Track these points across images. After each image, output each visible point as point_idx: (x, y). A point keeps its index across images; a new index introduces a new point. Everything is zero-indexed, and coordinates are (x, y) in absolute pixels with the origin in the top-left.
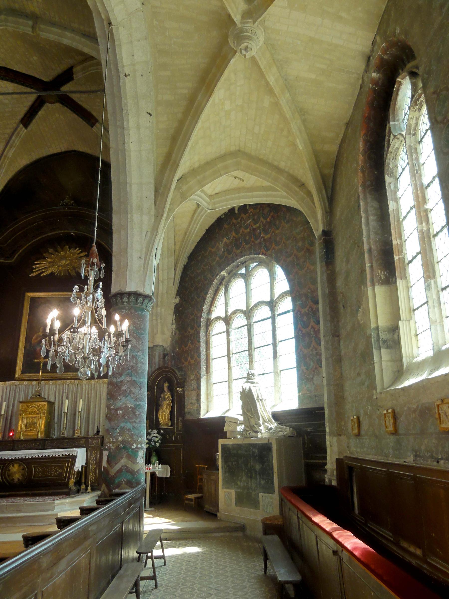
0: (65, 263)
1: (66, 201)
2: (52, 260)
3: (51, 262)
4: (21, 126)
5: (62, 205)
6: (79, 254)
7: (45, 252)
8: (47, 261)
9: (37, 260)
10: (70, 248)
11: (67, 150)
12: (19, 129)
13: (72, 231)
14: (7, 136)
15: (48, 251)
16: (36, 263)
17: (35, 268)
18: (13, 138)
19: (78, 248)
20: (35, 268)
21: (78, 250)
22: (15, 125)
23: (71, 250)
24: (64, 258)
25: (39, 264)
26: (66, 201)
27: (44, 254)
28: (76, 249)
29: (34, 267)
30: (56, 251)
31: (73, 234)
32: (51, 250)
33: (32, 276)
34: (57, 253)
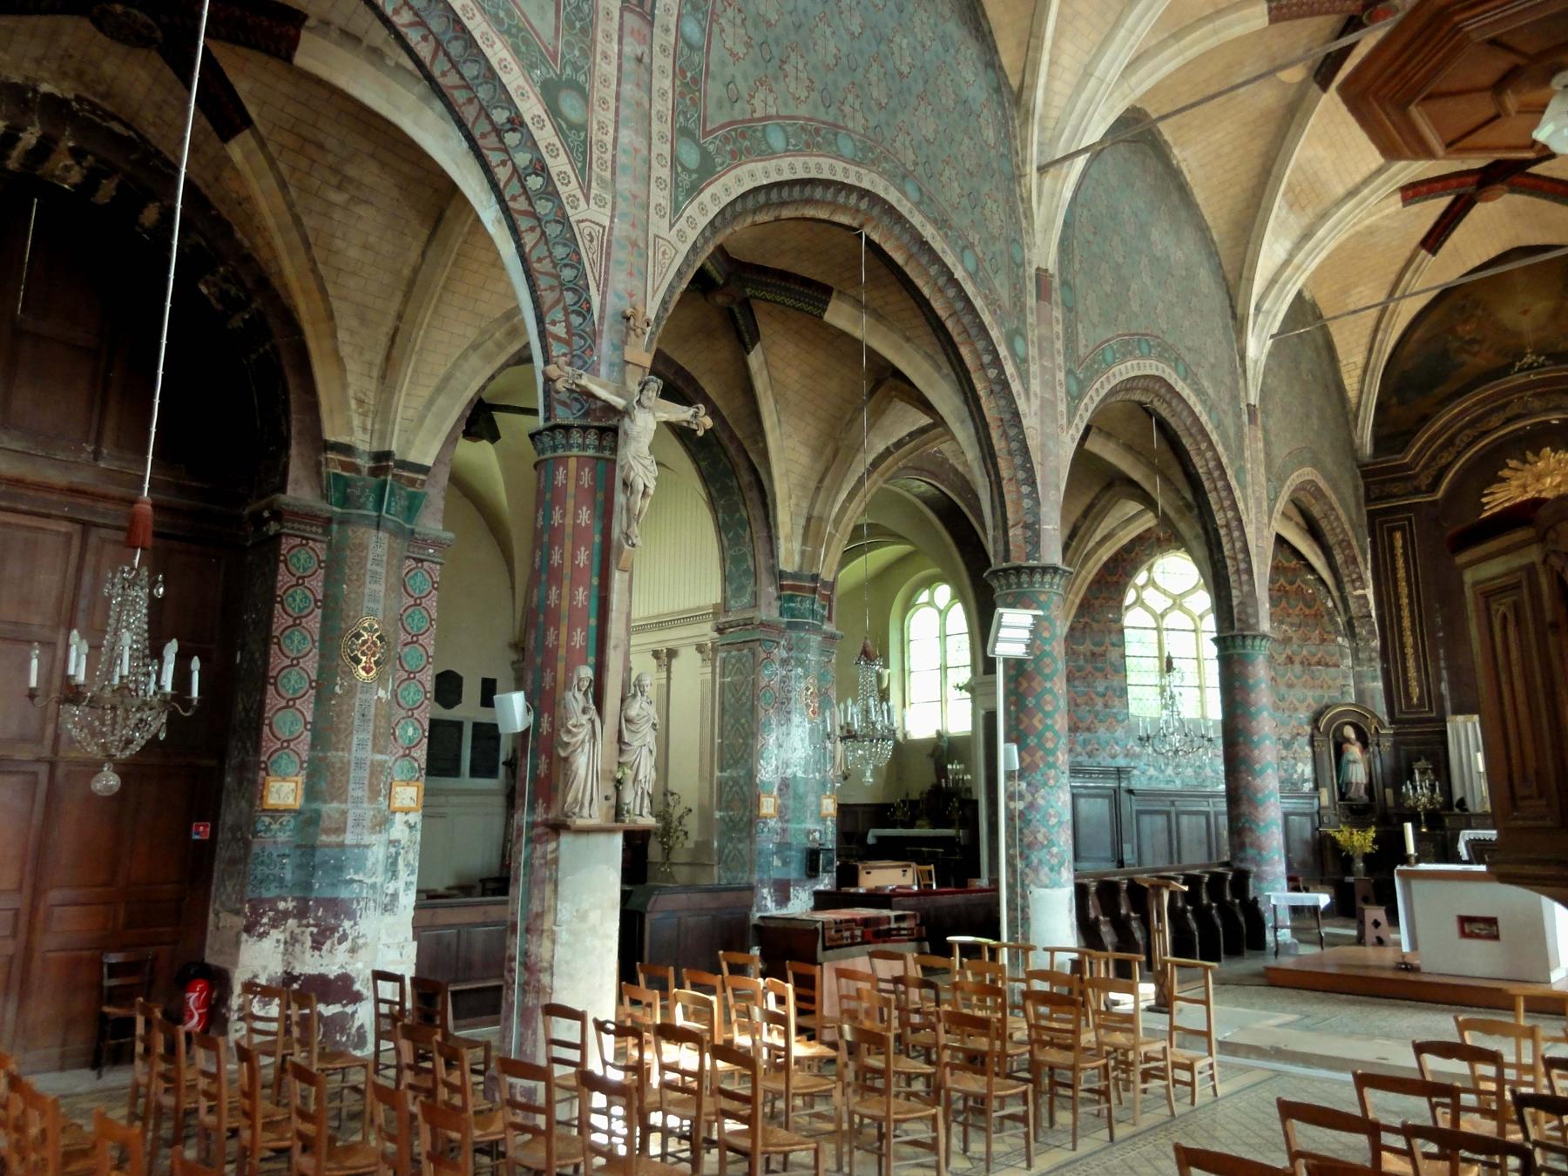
1: (1529, 359)
4: (1423, 252)
5: (1520, 371)
9: (1489, 485)
10: (1555, 451)
11: (1500, 251)
12: (1418, 260)
14: (1393, 277)
15: (1506, 466)
18: (1407, 276)
22: (1408, 254)
24: (1551, 473)
26: (1529, 359)
29: (1484, 500)
30: (1525, 461)
32: (1513, 463)
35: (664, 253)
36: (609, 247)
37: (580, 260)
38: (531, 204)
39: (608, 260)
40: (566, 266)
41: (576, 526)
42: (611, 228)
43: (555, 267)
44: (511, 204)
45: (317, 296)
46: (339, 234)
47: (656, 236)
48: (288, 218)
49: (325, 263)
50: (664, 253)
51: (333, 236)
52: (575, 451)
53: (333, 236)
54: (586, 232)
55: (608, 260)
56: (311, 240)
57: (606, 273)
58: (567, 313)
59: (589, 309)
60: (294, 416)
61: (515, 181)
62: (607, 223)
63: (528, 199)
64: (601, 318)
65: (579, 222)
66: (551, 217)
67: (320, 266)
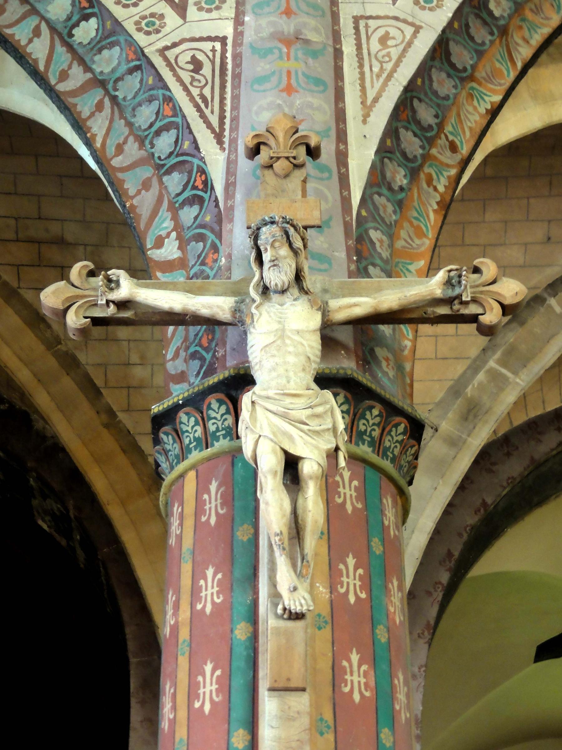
35: (384, 40)
36: (237, 63)
37: (177, 111)
38: (88, 69)
39: (236, 86)
40: (158, 133)
41: (196, 616)
42: (238, 35)
43: (141, 141)
44: (61, 87)
45: (122, 460)
46: (134, 358)
47: (356, 20)
48: (52, 362)
49: (128, 410)
50: (384, 40)
51: (128, 364)
52: (195, 456)
53: (128, 364)
54: (186, 58)
55: (236, 86)
56: (99, 382)
57: (235, 107)
58: (174, 210)
59: (208, 185)
60: (133, 660)
61: (60, 49)
62: (228, 30)
63: (82, 62)
64: (229, 186)
65: (162, 52)
66: (124, 68)
67: (121, 416)
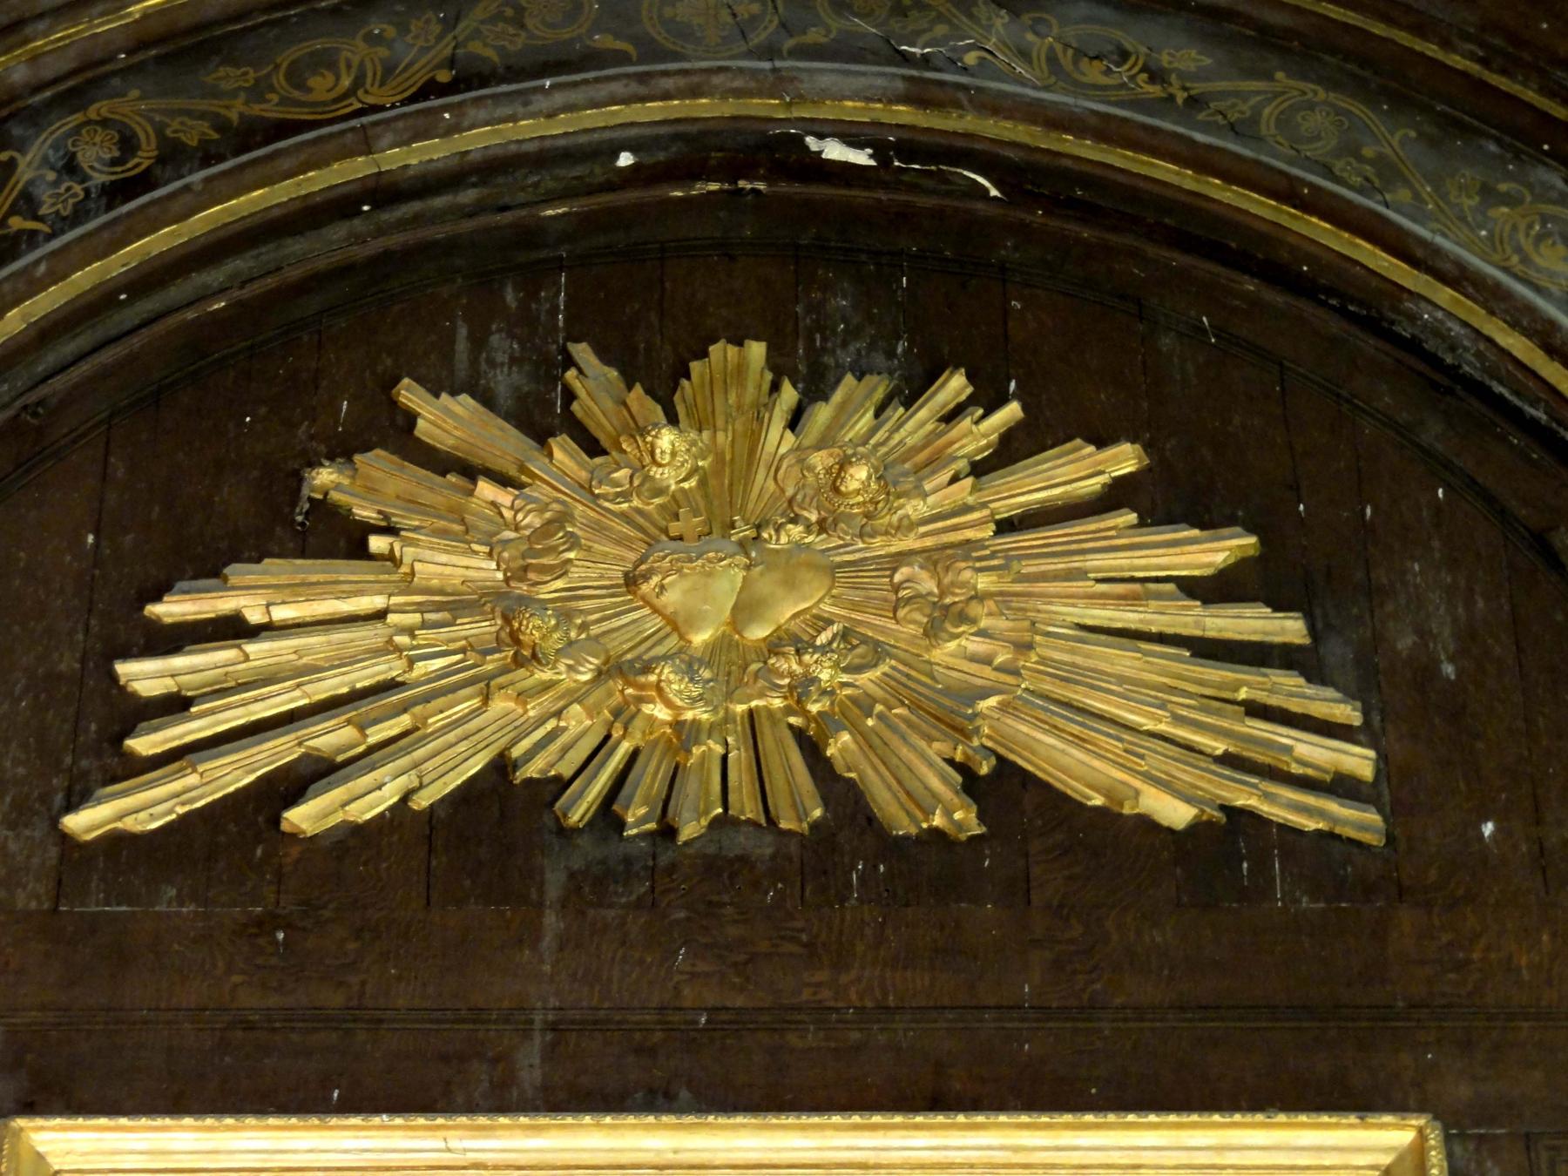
0: (745, 610)
2: (483, 569)
3: (457, 605)
6: (980, 469)
7: (343, 451)
8: (408, 584)
13: (852, 110)
16: (172, 609)
17: (176, 705)
19: (955, 386)
20: (176, 705)
21: (951, 416)
23: (822, 414)
25: (233, 629)
27: (325, 476)
28: (910, 393)
31: (834, 151)
33: (117, 843)
34: (563, 452)
